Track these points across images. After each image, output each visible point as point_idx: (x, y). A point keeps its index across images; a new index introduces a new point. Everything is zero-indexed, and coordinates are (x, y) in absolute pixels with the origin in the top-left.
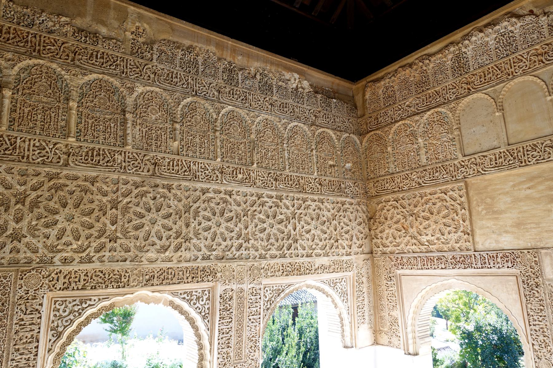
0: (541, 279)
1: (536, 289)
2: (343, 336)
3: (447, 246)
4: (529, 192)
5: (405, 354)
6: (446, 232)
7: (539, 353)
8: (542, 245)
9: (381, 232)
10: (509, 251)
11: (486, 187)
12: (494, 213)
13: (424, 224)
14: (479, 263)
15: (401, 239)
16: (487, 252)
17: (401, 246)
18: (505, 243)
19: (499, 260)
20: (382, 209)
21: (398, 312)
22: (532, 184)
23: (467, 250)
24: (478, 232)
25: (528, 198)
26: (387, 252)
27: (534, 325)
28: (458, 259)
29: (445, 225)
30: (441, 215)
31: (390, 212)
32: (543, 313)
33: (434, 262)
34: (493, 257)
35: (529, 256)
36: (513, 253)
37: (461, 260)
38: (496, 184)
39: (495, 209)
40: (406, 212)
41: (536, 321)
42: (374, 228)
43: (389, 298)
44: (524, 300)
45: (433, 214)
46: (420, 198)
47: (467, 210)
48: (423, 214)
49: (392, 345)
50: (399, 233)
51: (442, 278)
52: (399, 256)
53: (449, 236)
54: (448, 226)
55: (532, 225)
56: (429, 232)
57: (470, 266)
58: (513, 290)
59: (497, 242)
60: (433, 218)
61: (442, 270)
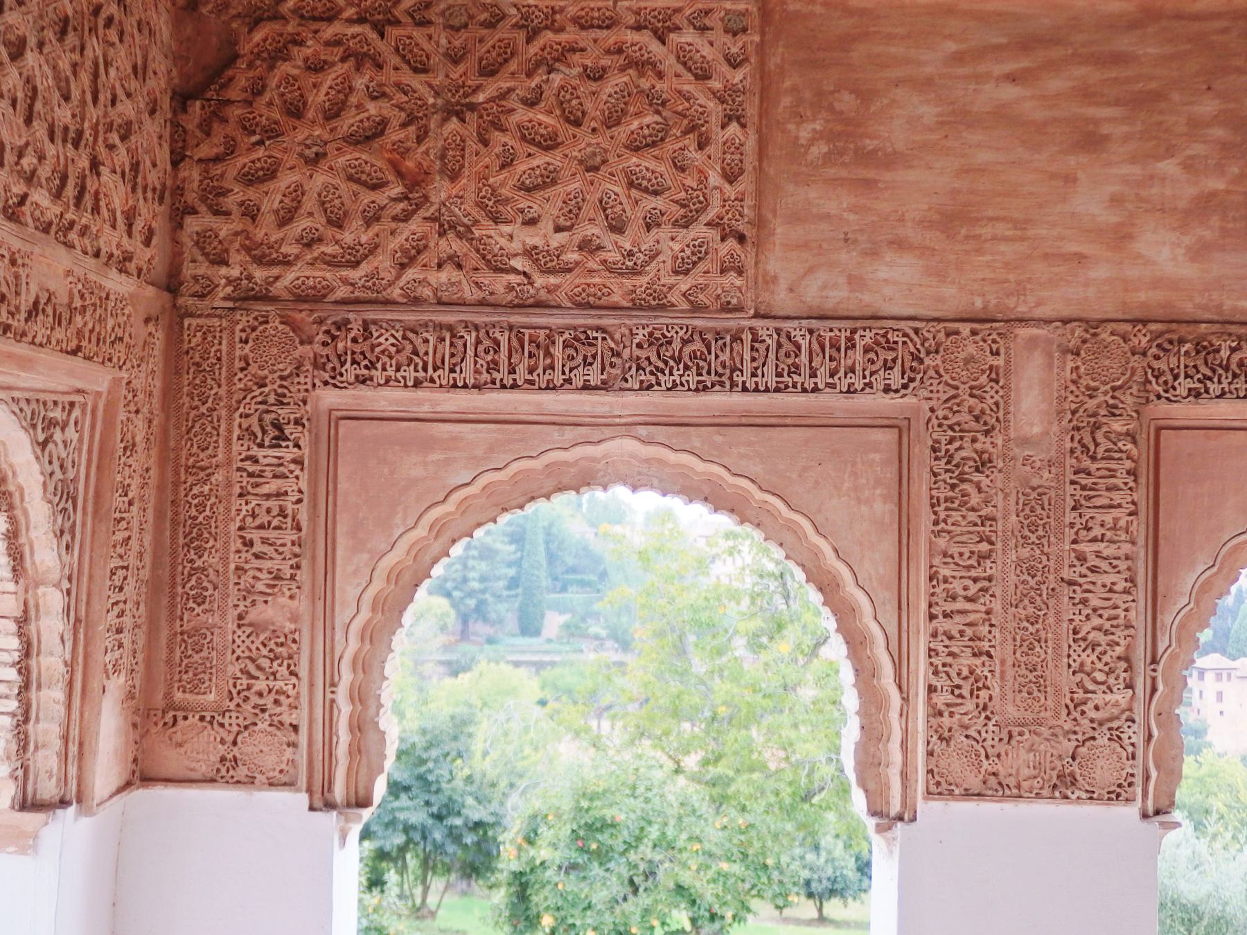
0: (1000, 442)
1: (977, 477)
2: (23, 742)
3: (628, 283)
4: (1009, 92)
5: (312, 808)
6: (636, 216)
7: (946, 721)
8: (1022, 309)
9: (250, 179)
10: (906, 326)
11: (846, 42)
12: (857, 154)
13: (521, 167)
14: (770, 369)
15: (376, 228)
16: (814, 324)
17: (365, 268)
18: (888, 291)
19: (858, 356)
20: (279, 53)
21: (302, 605)
22: (1024, 63)
23: (727, 308)
24: (781, 231)
25: (1002, 116)
26: (279, 288)
27: (946, 615)
28: (676, 345)
29: (631, 184)
30: (622, 132)
31: (329, 79)
32: (989, 568)
33: (548, 354)
34: (835, 346)
35: (971, 349)
36: (916, 331)
37: (688, 350)
38: (890, 37)
39: (870, 144)
40: (423, 90)
41: (954, 598)
42: (205, 151)
43: (255, 536)
44: (925, 519)
45: (577, 123)
46: (521, 36)
47: (751, 131)
48: (522, 115)
49: (242, 772)
50: (367, 197)
51: (570, 434)
52: (356, 319)
53: (648, 242)
54: (646, 190)
55: (1001, 229)
56: (548, 207)
57: (727, 379)
58: (878, 482)
59: (856, 282)
60: (585, 142)
61: (585, 397)
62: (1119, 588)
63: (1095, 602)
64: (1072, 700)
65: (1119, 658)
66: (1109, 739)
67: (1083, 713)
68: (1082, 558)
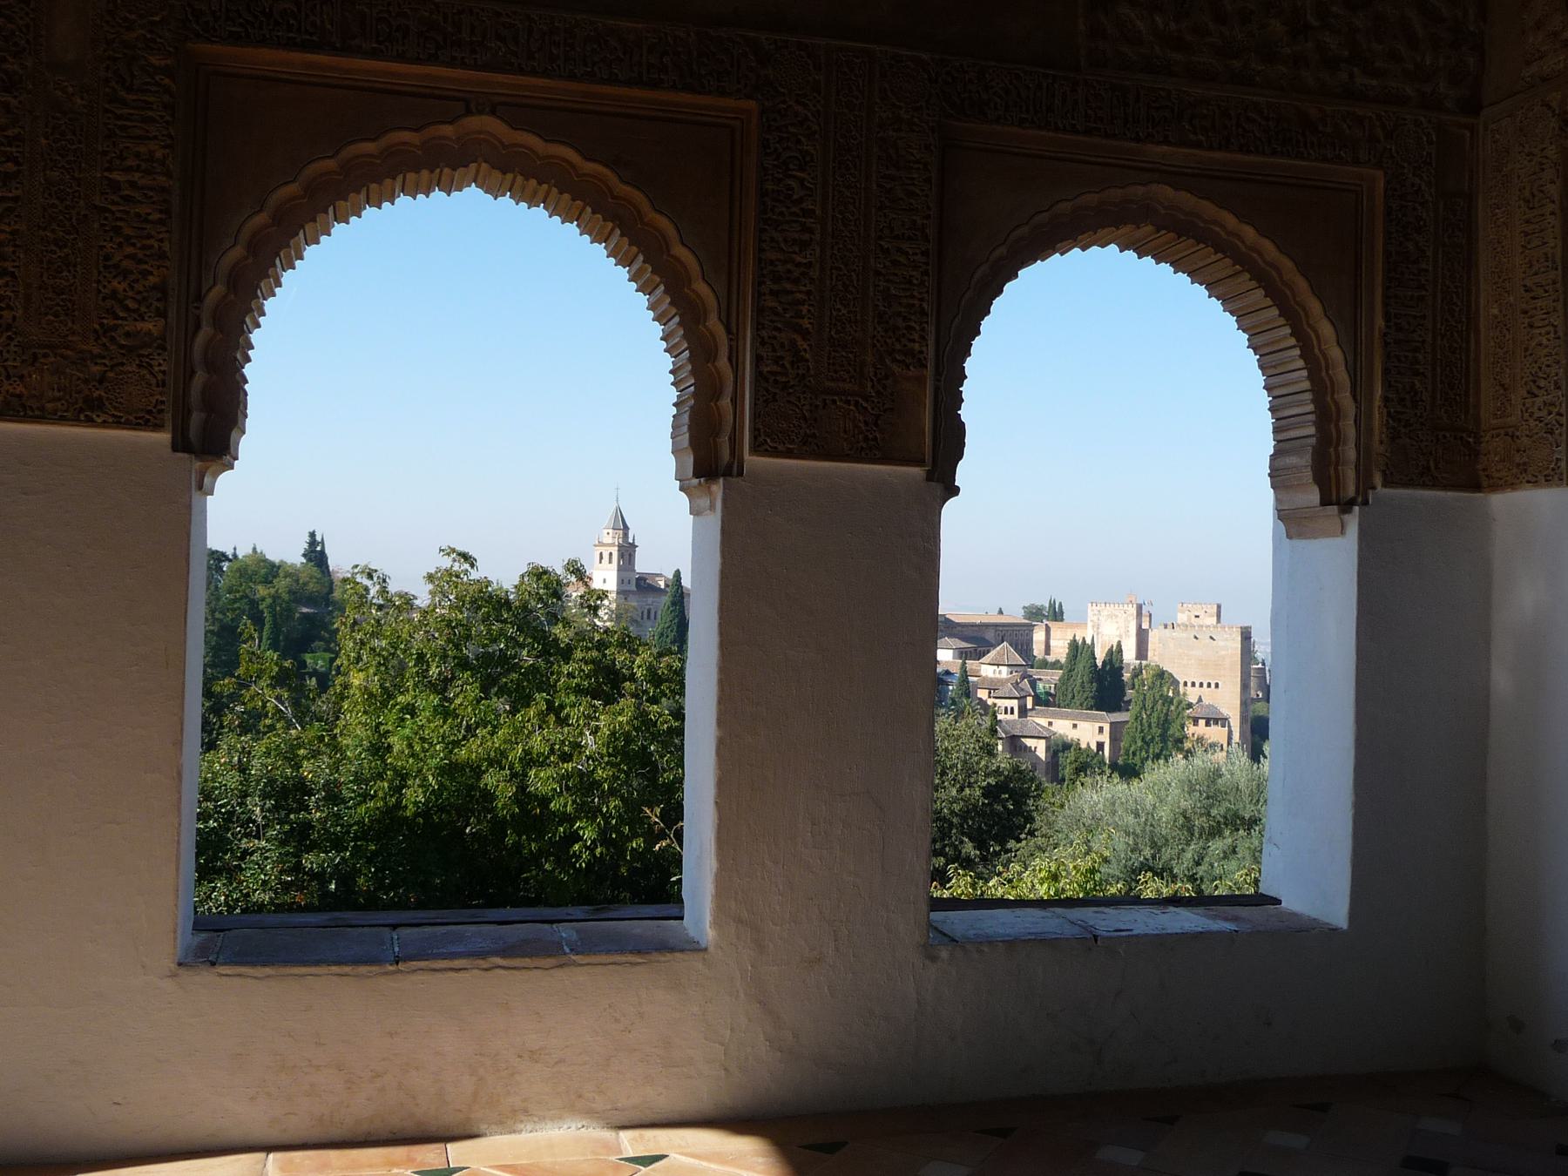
62: (155, 216)
63: (128, 231)
64: (102, 325)
65: (154, 288)
66: (139, 366)
67: (112, 339)
68: (115, 186)
